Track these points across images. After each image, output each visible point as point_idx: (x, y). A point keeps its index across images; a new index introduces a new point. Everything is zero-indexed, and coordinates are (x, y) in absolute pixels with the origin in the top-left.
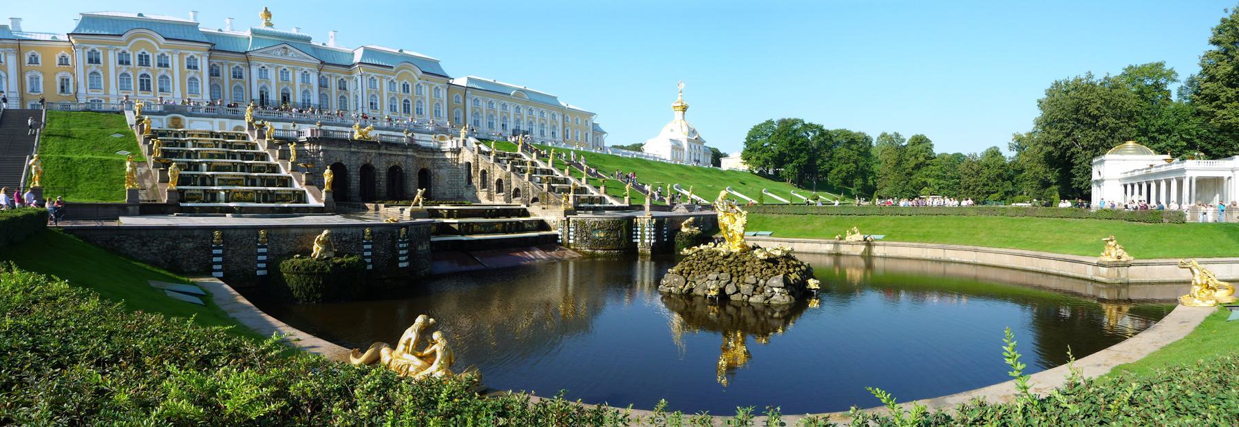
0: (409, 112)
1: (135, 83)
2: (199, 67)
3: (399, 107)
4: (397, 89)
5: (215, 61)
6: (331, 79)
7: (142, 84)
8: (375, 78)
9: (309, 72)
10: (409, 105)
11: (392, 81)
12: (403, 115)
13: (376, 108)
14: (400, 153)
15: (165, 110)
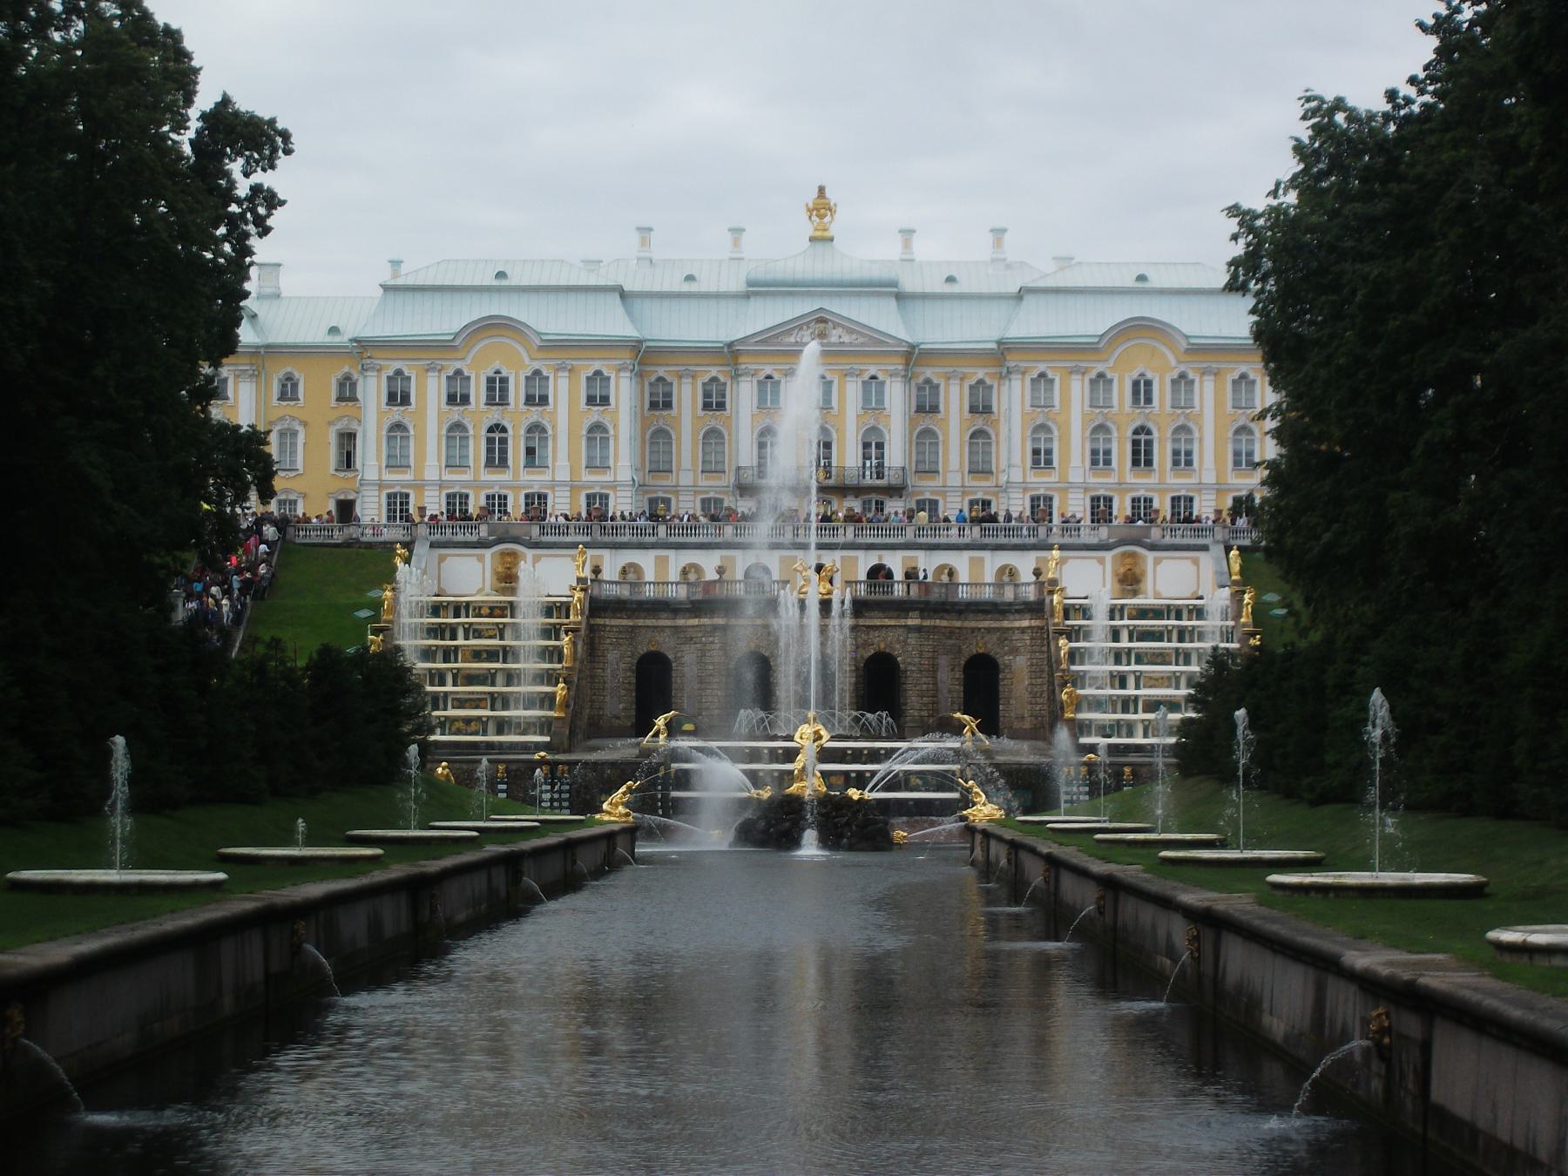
0: (1149, 463)
1: (477, 449)
2: (612, 400)
3: (1121, 452)
4: (1115, 402)
5: (661, 374)
6: (947, 385)
7: (490, 451)
8: (1050, 376)
9: (881, 377)
10: (1149, 443)
11: (1101, 375)
12: (1130, 478)
13: (1049, 462)
14: (892, 622)
15: (489, 535)
